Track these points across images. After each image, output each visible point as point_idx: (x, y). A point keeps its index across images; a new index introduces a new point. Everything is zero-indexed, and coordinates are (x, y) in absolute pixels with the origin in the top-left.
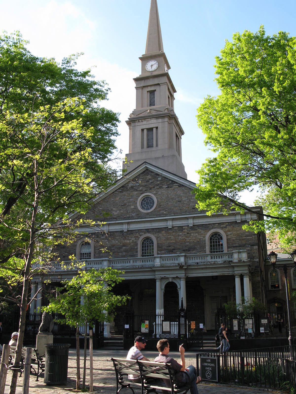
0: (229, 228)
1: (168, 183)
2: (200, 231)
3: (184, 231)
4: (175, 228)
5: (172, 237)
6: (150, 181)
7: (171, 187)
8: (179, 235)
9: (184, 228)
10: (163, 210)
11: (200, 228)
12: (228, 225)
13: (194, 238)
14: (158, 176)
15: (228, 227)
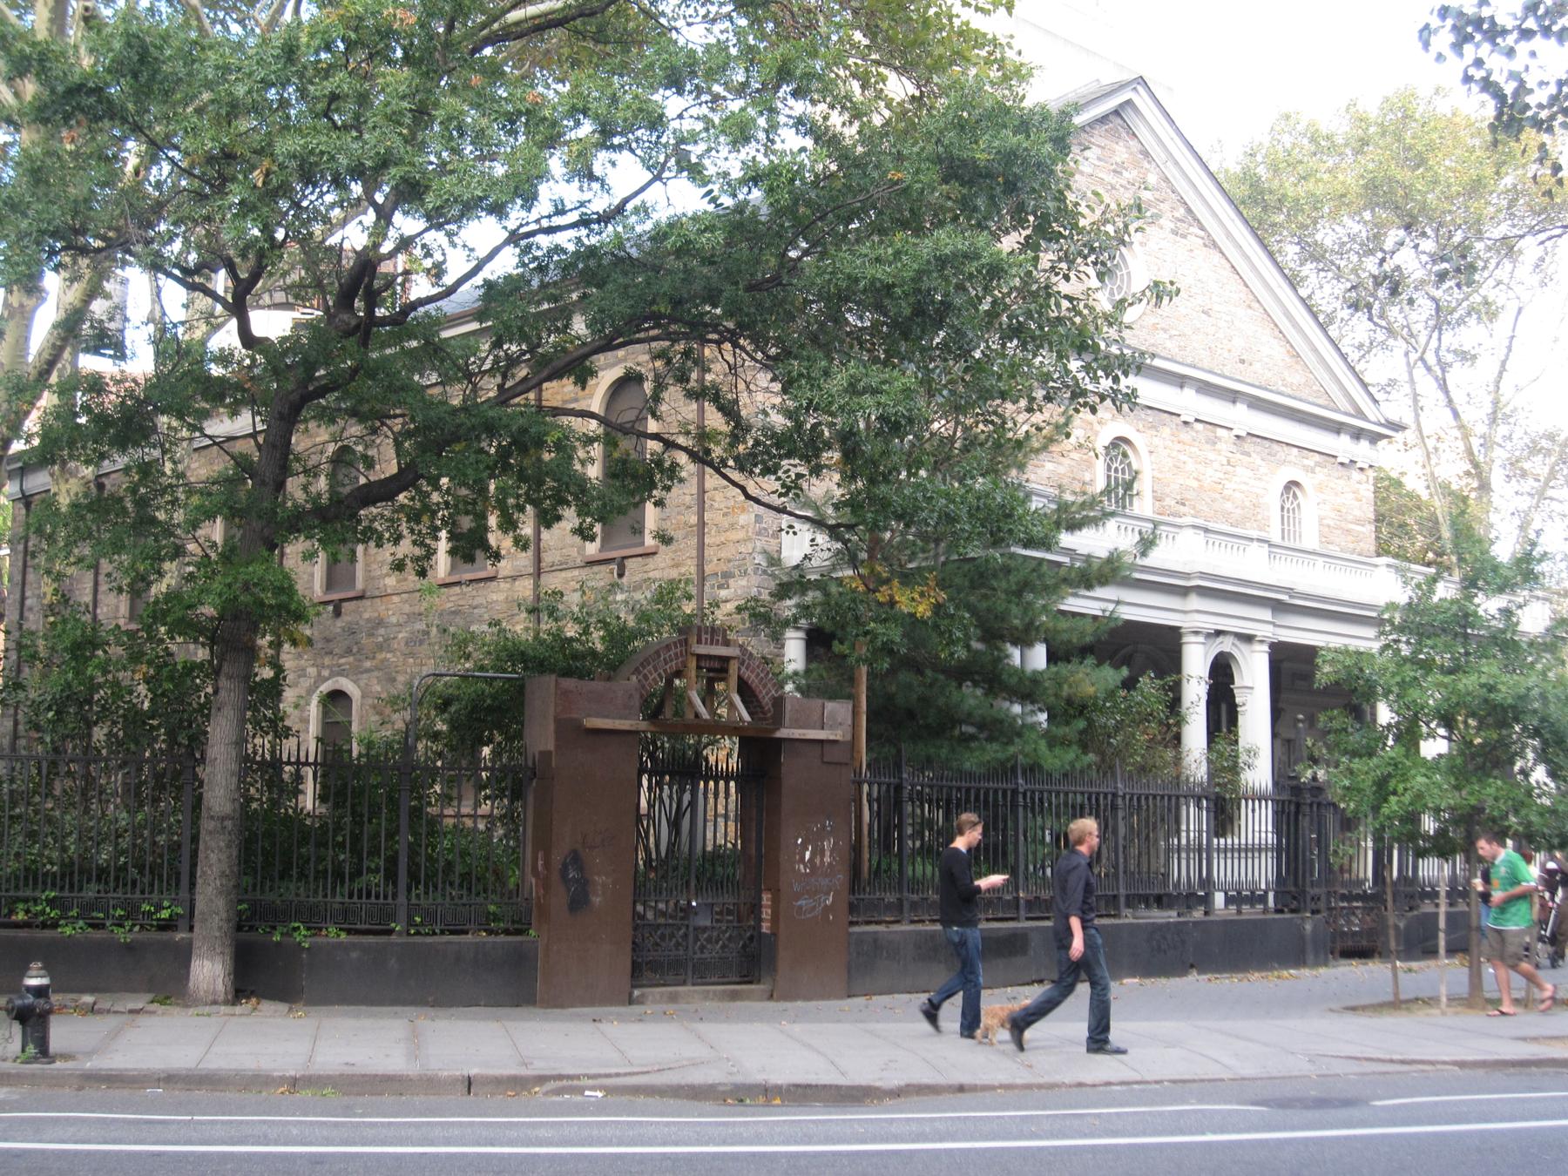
0: (1321, 474)
1: (1177, 215)
2: (1258, 462)
3: (1218, 446)
4: (1199, 426)
5: (1190, 466)
6: (1125, 174)
7: (1184, 236)
8: (1207, 462)
9: (1220, 432)
10: (1165, 330)
11: (1259, 449)
12: (1318, 464)
13: (1244, 487)
14: (1146, 165)
15: (1318, 469)
